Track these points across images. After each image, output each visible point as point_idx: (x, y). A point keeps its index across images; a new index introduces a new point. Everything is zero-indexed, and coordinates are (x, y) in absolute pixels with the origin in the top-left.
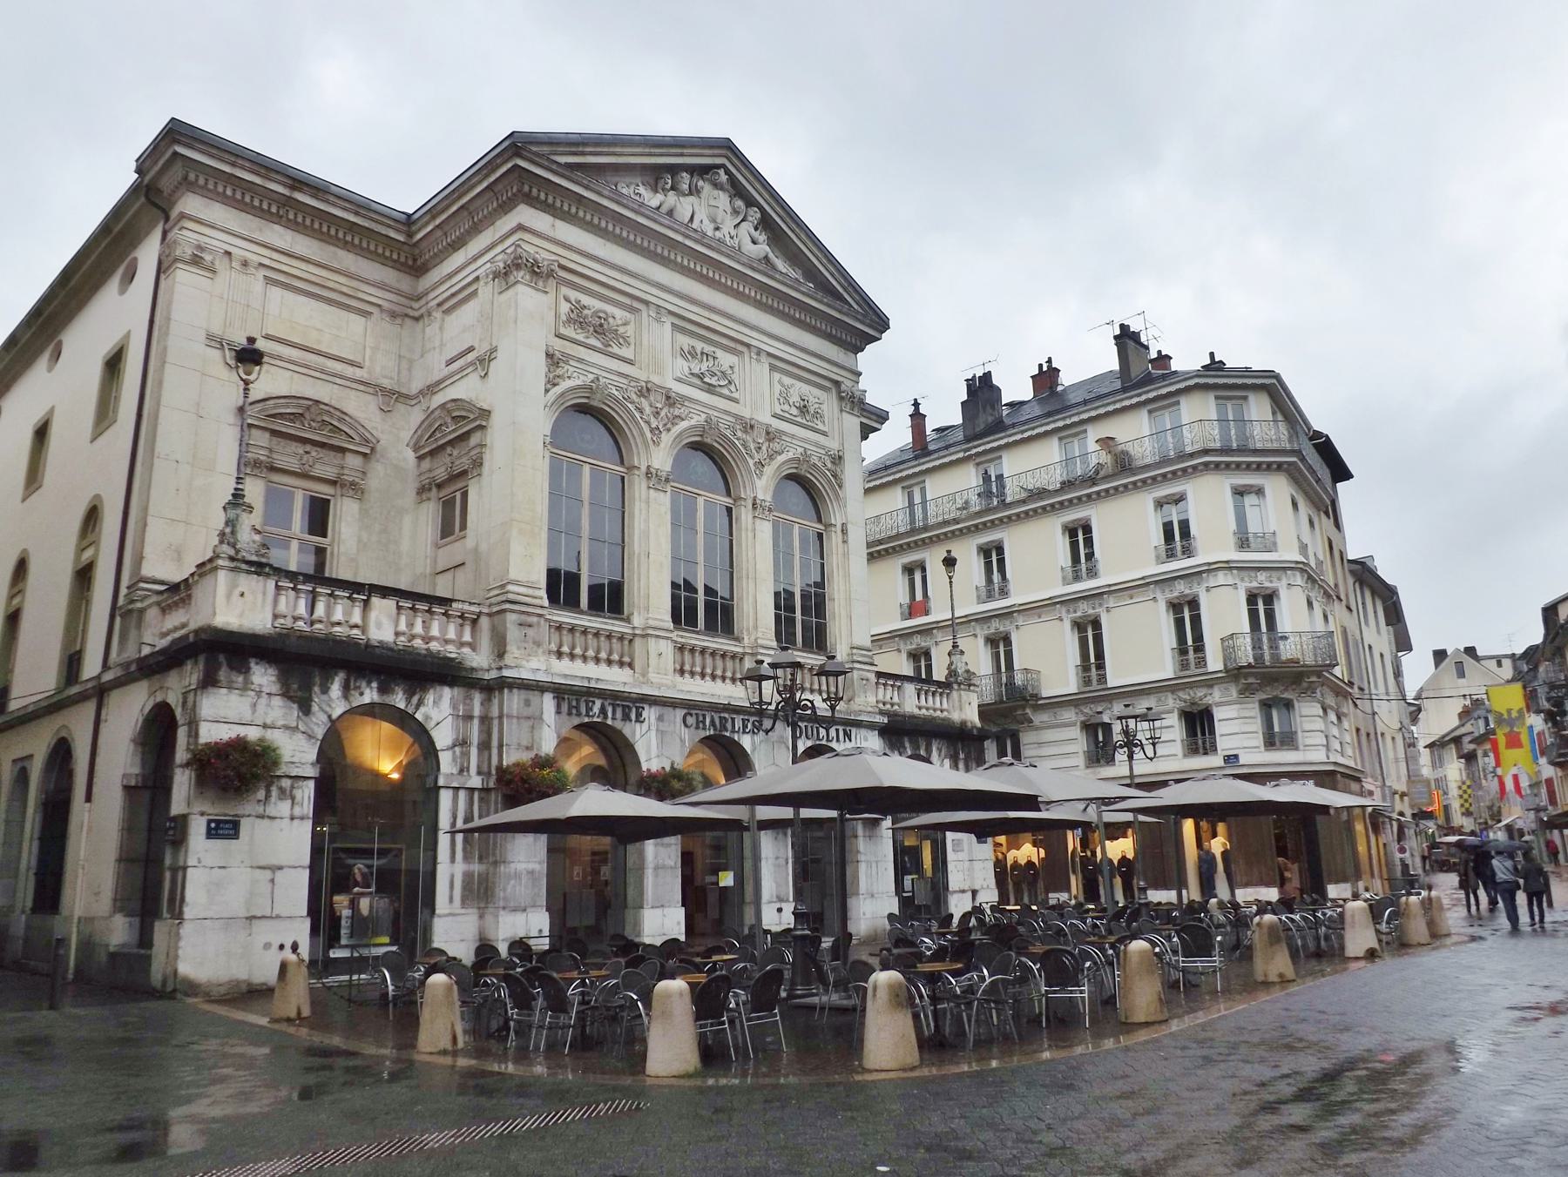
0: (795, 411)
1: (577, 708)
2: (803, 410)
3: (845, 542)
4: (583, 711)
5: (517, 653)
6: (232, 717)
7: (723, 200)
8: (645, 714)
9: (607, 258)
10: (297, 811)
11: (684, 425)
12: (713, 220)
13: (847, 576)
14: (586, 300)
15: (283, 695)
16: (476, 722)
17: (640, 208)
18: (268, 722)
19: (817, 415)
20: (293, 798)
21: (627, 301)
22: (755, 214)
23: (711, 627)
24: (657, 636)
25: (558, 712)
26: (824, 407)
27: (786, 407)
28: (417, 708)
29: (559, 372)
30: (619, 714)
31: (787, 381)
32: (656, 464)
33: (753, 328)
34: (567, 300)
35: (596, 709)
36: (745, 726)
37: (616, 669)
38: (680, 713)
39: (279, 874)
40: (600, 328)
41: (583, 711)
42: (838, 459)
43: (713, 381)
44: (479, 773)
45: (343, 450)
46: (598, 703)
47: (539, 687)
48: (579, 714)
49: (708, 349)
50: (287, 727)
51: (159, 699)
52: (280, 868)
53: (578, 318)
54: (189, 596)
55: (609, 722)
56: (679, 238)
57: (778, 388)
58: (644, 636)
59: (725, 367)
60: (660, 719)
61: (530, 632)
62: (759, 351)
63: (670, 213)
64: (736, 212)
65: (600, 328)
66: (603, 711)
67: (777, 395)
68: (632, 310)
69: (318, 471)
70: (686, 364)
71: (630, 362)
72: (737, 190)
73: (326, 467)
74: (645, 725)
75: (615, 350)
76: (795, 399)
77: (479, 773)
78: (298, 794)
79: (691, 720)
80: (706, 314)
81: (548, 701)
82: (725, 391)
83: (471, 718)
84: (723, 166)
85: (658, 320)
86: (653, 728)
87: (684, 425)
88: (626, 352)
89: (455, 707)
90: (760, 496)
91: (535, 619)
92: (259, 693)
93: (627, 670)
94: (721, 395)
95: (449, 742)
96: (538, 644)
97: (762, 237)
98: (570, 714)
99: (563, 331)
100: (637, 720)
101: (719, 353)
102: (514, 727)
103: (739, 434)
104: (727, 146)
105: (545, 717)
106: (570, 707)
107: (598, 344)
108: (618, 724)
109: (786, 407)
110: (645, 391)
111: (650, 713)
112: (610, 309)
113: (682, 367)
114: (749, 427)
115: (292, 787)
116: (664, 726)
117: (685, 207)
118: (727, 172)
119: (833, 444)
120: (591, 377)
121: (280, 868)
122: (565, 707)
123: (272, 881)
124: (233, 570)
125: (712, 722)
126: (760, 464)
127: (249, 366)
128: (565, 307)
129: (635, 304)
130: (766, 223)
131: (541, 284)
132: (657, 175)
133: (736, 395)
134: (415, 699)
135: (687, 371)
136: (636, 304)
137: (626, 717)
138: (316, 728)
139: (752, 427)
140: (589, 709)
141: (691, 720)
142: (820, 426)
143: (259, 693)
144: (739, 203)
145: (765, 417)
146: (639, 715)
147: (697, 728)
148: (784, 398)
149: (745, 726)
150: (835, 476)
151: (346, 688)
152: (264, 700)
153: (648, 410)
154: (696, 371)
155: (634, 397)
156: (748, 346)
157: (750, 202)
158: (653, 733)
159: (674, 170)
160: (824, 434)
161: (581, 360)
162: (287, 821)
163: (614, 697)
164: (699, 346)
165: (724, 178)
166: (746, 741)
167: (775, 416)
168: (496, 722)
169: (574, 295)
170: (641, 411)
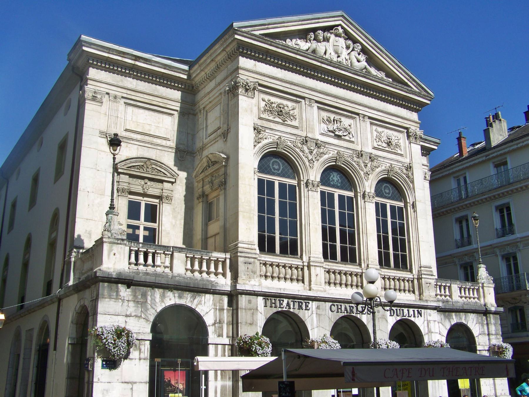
0: (385, 145)
2: (389, 144)
5: (244, 277)
6: (111, 311)
7: (341, 42)
8: (310, 306)
10: (142, 356)
11: (326, 157)
12: (336, 52)
13: (417, 229)
14: (273, 99)
15: (134, 301)
16: (225, 311)
17: (298, 51)
18: (128, 313)
19: (397, 146)
20: (140, 350)
23: (344, 259)
25: (265, 306)
26: (401, 141)
27: (380, 143)
28: (197, 306)
29: (260, 136)
31: (380, 129)
32: (312, 178)
34: (263, 100)
36: (363, 311)
37: (295, 283)
38: (329, 304)
39: (135, 385)
42: (409, 168)
43: (340, 133)
44: (228, 337)
45: (162, 181)
47: (256, 294)
48: (276, 307)
49: (337, 117)
50: (136, 316)
51: (82, 303)
52: (135, 383)
53: (269, 109)
54: (93, 255)
55: (292, 310)
57: (375, 134)
59: (347, 126)
60: (318, 308)
61: (250, 266)
64: (348, 47)
66: (288, 305)
67: (375, 137)
69: (151, 192)
70: (325, 126)
71: (296, 128)
72: (348, 36)
73: (154, 189)
74: (310, 311)
75: (289, 122)
76: (384, 138)
77: (228, 337)
78: (142, 347)
80: (335, 100)
82: (347, 138)
83: (223, 309)
84: (340, 25)
85: (310, 106)
87: (326, 157)
88: (295, 123)
89: (215, 305)
90: (368, 190)
91: (252, 260)
92: (123, 301)
93: (301, 284)
94: (345, 140)
96: (254, 272)
97: (362, 57)
99: (262, 116)
101: (343, 119)
102: (244, 314)
103: (355, 159)
105: (259, 309)
106: (271, 303)
108: (296, 311)
109: (380, 143)
110: (305, 141)
111: (313, 305)
112: (285, 102)
113: (324, 127)
114: (360, 155)
115: (140, 344)
116: (319, 312)
117: (321, 47)
118: (343, 28)
120: (277, 137)
121: (135, 383)
122: (269, 303)
123: (132, 389)
124: (110, 243)
125: (346, 308)
126: (367, 174)
127: (115, 148)
128: (263, 104)
129: (298, 98)
130: (364, 51)
134: (196, 301)
135: (326, 129)
136: (298, 99)
138: (149, 316)
139: (362, 155)
141: (334, 308)
142: (399, 152)
143: (123, 301)
144: (350, 42)
145: (369, 149)
146: (307, 306)
147: (338, 312)
148: (379, 138)
150: (408, 177)
151: (163, 297)
152: (126, 303)
153: (307, 151)
154: (331, 129)
155: (300, 145)
156: (358, 114)
157: (355, 41)
158: (314, 315)
160: (401, 155)
162: (138, 360)
163: (293, 297)
164: (332, 116)
165: (341, 30)
167: (374, 148)
169: (267, 97)
170: (303, 152)
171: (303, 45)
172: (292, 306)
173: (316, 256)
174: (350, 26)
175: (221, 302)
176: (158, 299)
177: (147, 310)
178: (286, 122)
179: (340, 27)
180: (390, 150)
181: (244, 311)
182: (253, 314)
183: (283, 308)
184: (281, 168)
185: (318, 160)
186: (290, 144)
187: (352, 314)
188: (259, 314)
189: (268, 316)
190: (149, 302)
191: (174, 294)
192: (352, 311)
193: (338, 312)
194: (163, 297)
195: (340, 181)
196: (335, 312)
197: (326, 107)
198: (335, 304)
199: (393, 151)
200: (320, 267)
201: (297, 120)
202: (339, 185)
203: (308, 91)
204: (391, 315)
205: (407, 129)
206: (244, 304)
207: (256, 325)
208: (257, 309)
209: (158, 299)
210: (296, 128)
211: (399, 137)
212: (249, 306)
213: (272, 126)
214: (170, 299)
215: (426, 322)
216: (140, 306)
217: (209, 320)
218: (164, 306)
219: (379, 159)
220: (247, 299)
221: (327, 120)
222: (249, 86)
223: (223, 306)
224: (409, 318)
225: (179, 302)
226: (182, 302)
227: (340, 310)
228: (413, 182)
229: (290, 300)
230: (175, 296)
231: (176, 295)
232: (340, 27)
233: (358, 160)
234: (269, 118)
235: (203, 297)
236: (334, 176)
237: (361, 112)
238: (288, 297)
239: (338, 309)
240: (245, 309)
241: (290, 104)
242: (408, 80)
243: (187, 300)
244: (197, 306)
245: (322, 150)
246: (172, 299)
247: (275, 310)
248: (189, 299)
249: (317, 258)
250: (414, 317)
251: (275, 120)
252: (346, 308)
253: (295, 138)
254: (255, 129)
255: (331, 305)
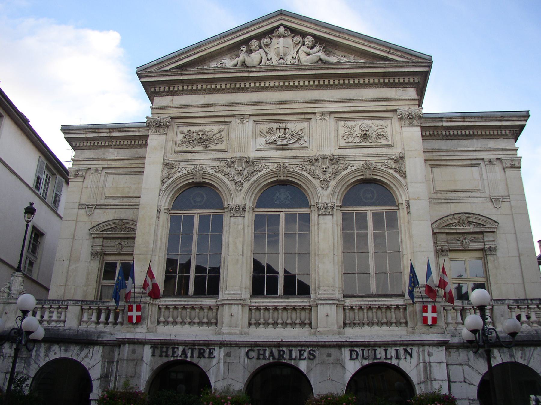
0: (357, 140)
1: (166, 352)
3: (408, 213)
4: (170, 352)
7: (289, 41)
8: (216, 353)
9: (206, 103)
17: (226, 70)
21: (222, 119)
22: (309, 40)
24: (229, 304)
25: (153, 355)
28: (83, 359)
29: (173, 170)
30: (196, 354)
31: (350, 123)
33: (316, 102)
34: (182, 133)
35: (179, 352)
36: (301, 355)
38: (244, 351)
40: (203, 140)
41: (170, 352)
43: (284, 142)
46: (181, 349)
48: (167, 356)
53: (188, 140)
55: (189, 359)
56: (246, 75)
58: (222, 305)
60: (228, 355)
62: (323, 114)
63: (244, 63)
65: (203, 140)
66: (184, 353)
68: (225, 123)
70: (263, 139)
71: (224, 151)
72: (294, 32)
74: (215, 361)
75: (213, 147)
76: (358, 131)
79: (252, 354)
80: (278, 106)
81: (147, 351)
84: (281, 25)
86: (222, 361)
88: (220, 147)
95: (99, 376)
98: (161, 356)
99: (178, 149)
100: (209, 357)
101: (291, 126)
104: (281, 13)
105: (144, 359)
106: (162, 352)
107: (201, 148)
108: (195, 360)
109: (350, 140)
112: (208, 128)
116: (228, 360)
117: (255, 57)
118: (285, 26)
119: (395, 152)
122: (157, 352)
125: (272, 354)
131: (162, 131)
132: (234, 49)
133: (306, 145)
134: (83, 354)
135: (263, 143)
136: (227, 119)
137: (201, 355)
140: (174, 352)
142: (384, 142)
144: (298, 38)
146: (210, 353)
147: (258, 358)
149: (301, 355)
150: (398, 171)
154: (271, 140)
157: (304, 35)
158: (222, 364)
159: (246, 42)
161: (187, 161)
163: (192, 345)
164: (275, 126)
165: (282, 30)
166: (303, 366)
167: (341, 148)
168: (115, 364)
169: (185, 129)
170: (228, 175)
171: (228, 62)
172: (189, 355)
173: (234, 292)
174: (294, 20)
175: (111, 353)
176: (42, 354)
177: (29, 365)
178: (209, 148)
179: (282, 27)
180: (368, 144)
181: (125, 362)
182: (136, 365)
183: (177, 357)
184: (205, 199)
185: (249, 180)
186: (210, 171)
187: (283, 361)
188: (145, 364)
189: (156, 367)
190: (33, 357)
191: (60, 347)
192: (281, 356)
193: (258, 358)
194: (48, 350)
195: (290, 197)
196: (254, 360)
197: (266, 118)
198: (255, 349)
199: (373, 144)
200: (238, 304)
201: (225, 143)
202: (287, 203)
203: (237, 108)
204: (351, 359)
205: (396, 111)
206: (126, 354)
207: (139, 377)
208: (142, 359)
209: (42, 354)
210: (224, 151)
211: (385, 125)
212: (135, 356)
213: (189, 156)
214: (55, 353)
215: (421, 365)
216: (23, 361)
217: (95, 373)
218: (48, 360)
219: (347, 159)
220: (131, 348)
221: (267, 132)
222: (157, 124)
223: (114, 358)
224: (388, 361)
225: (63, 355)
226: (68, 355)
227: (261, 357)
228: (405, 177)
229: (186, 348)
230: (60, 350)
231: (63, 348)
232: (282, 27)
233: (313, 167)
234: (187, 149)
235: (91, 350)
236: (280, 194)
237: (316, 110)
238: (185, 343)
239: (259, 354)
240: (127, 360)
241: (216, 128)
242: (388, 53)
243: (73, 353)
244: (83, 359)
245: (256, 167)
246: (57, 353)
247: (165, 360)
248: (75, 352)
249: (234, 294)
250: (398, 358)
251: (194, 149)
252: (272, 354)
253: (218, 162)
254: (166, 164)
255: (248, 351)
